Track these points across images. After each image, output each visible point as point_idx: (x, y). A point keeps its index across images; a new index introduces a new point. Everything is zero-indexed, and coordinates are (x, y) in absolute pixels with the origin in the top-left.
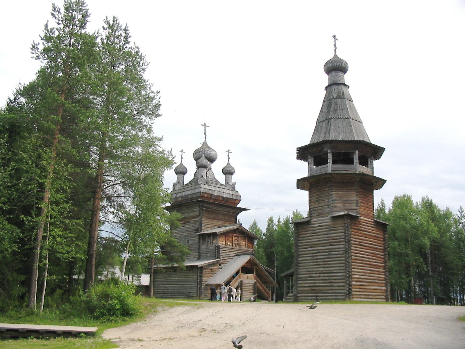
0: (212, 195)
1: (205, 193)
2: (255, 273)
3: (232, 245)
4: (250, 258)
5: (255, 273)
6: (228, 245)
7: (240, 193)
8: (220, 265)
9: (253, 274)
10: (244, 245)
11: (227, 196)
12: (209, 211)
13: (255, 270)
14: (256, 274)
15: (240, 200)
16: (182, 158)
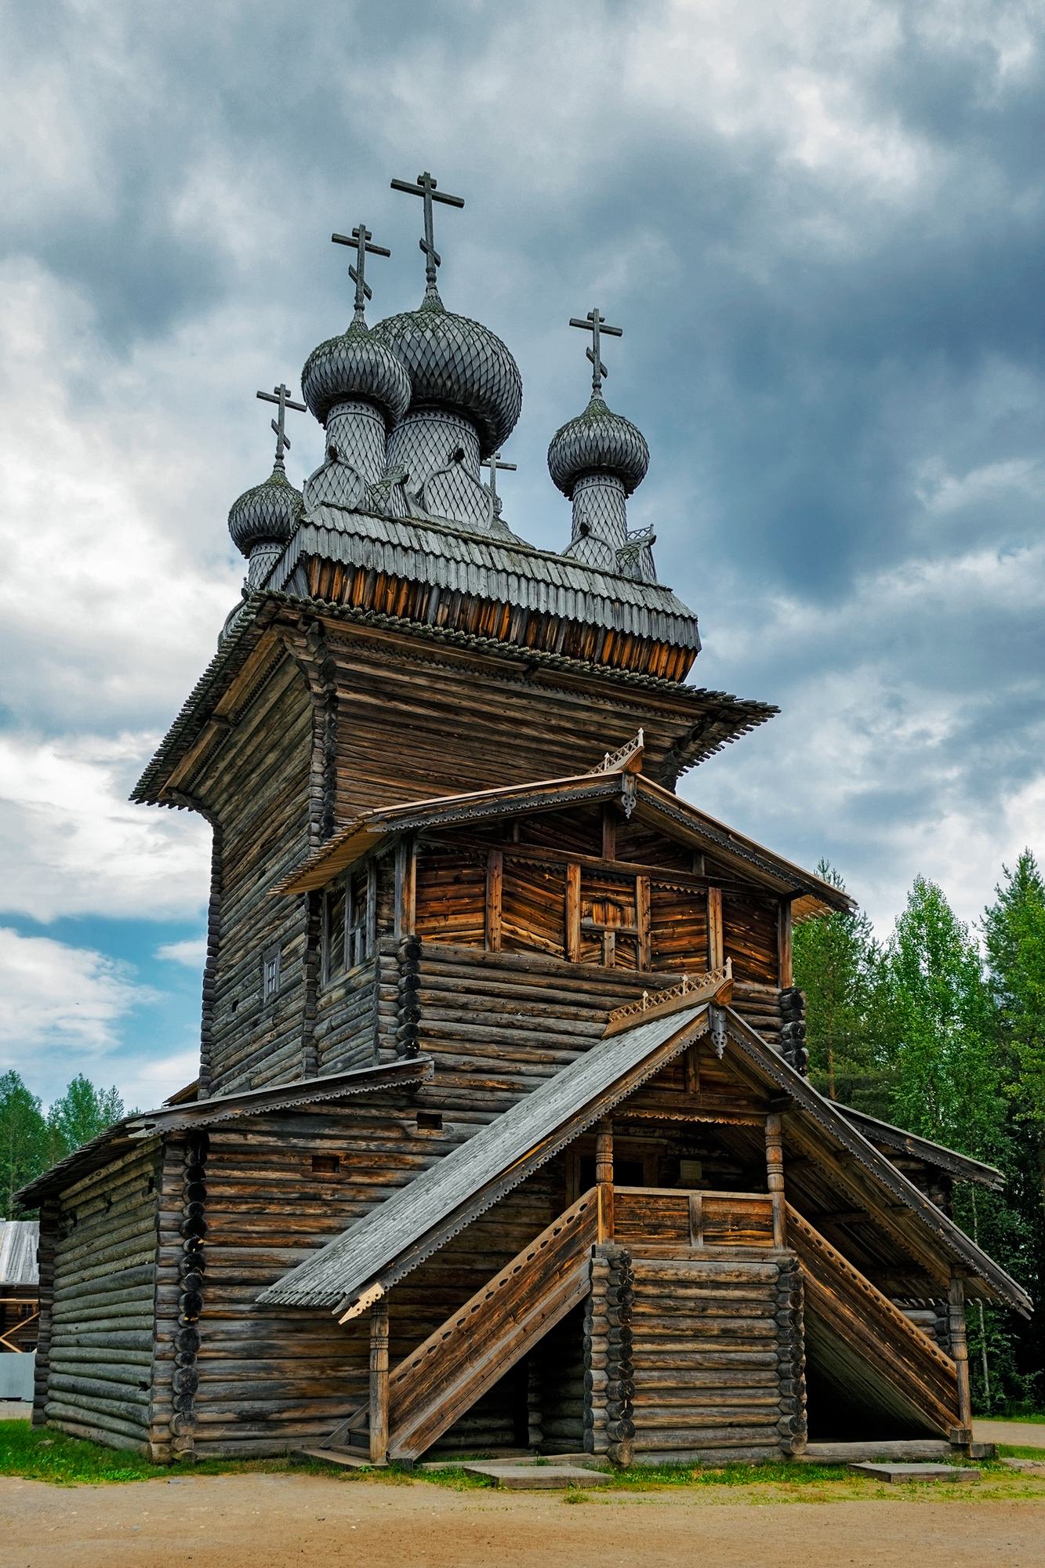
0: (416, 587)
1: (353, 571)
2: (775, 1180)
3: (565, 944)
4: (701, 1028)
5: (775, 1180)
6: (510, 943)
7: (686, 600)
8: (435, 1122)
9: (767, 1191)
10: (686, 953)
11: (566, 608)
12: (404, 722)
13: (773, 1154)
14: (789, 1192)
15: (689, 652)
16: (284, 442)
